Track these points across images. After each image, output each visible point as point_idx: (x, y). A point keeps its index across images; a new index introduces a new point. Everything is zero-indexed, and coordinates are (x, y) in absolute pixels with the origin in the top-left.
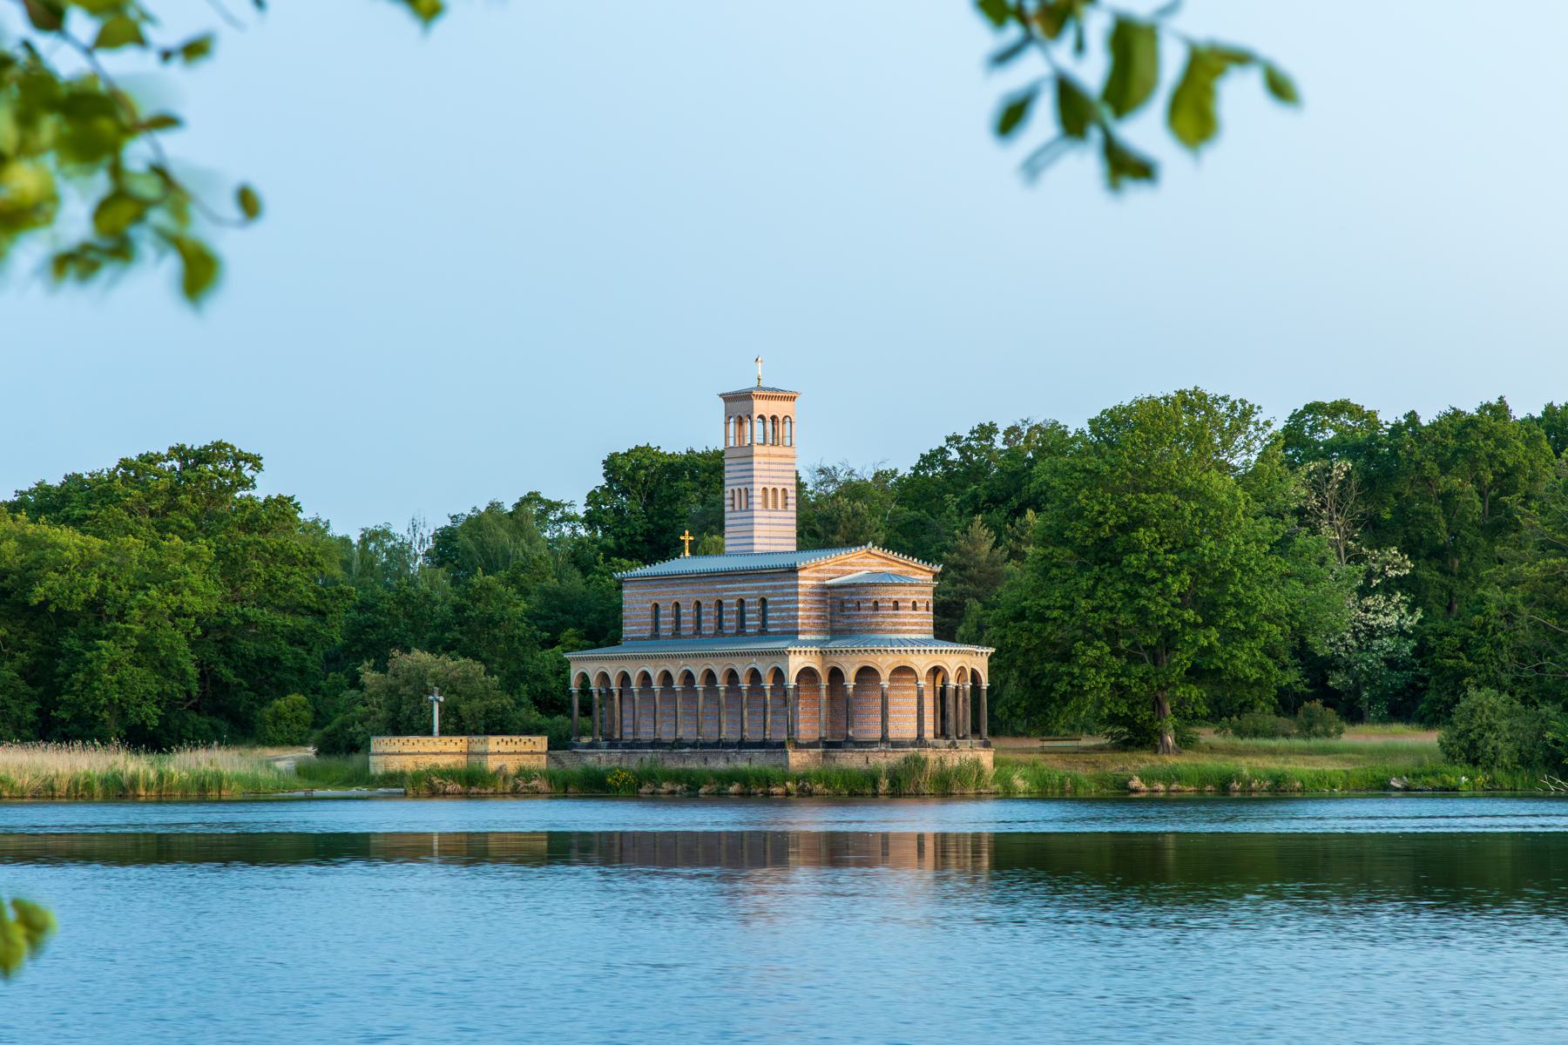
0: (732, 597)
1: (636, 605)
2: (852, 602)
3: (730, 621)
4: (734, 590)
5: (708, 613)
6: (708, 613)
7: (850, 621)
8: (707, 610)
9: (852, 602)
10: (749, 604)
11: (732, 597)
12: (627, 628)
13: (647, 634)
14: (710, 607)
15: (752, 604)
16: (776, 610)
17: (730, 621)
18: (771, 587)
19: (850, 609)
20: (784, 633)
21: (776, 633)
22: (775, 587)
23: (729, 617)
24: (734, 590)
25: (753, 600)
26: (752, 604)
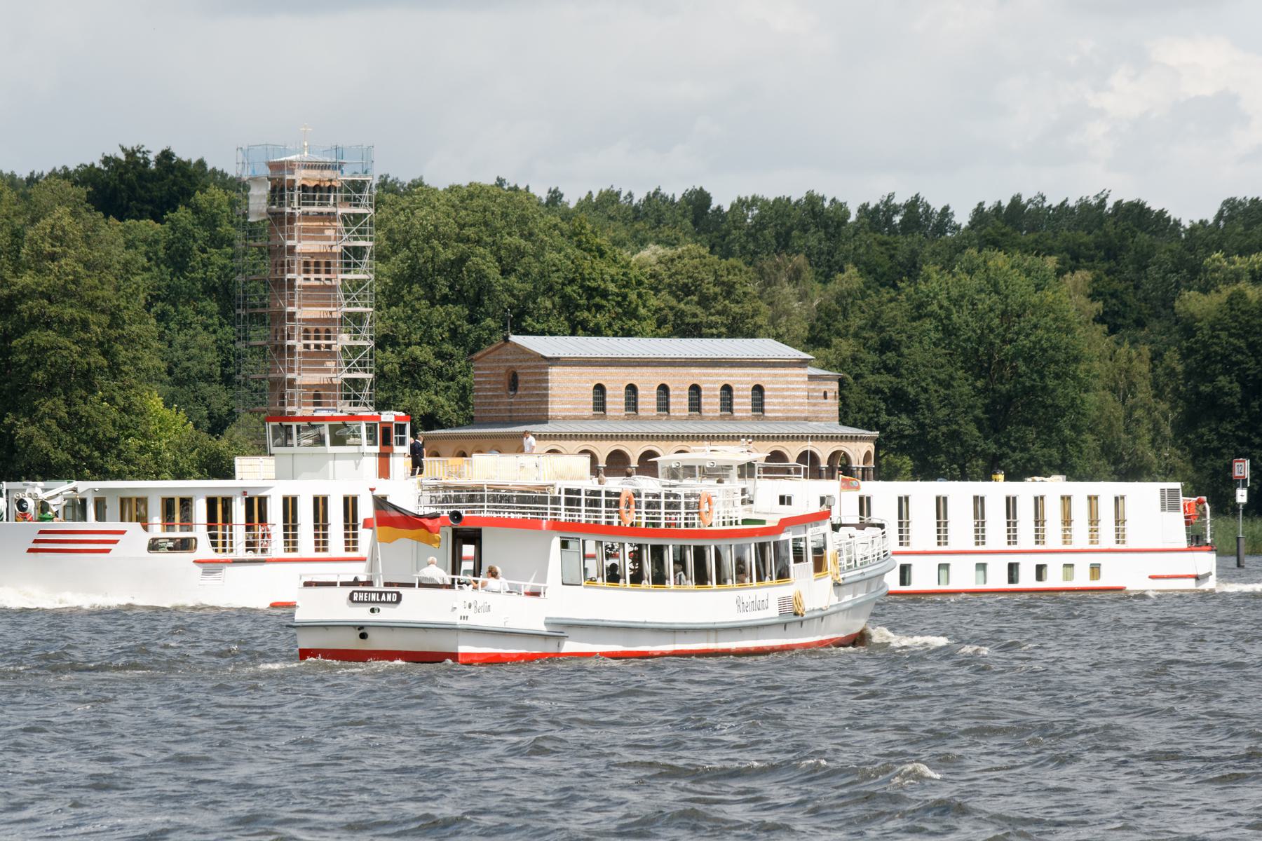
0: (714, 382)
1: (570, 385)
2: (819, 391)
3: (711, 404)
4: (717, 375)
5: (678, 396)
6: (678, 396)
7: (816, 408)
8: (677, 393)
9: (819, 391)
10: (738, 390)
11: (714, 382)
12: (555, 407)
13: (588, 410)
14: (682, 390)
15: (743, 390)
16: (776, 397)
17: (711, 404)
18: (769, 375)
19: (817, 397)
20: (787, 418)
21: (776, 419)
22: (775, 375)
23: (709, 400)
24: (717, 375)
25: (744, 386)
26: (743, 390)
